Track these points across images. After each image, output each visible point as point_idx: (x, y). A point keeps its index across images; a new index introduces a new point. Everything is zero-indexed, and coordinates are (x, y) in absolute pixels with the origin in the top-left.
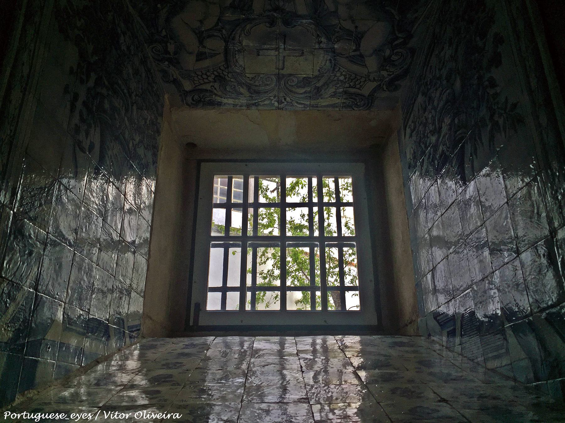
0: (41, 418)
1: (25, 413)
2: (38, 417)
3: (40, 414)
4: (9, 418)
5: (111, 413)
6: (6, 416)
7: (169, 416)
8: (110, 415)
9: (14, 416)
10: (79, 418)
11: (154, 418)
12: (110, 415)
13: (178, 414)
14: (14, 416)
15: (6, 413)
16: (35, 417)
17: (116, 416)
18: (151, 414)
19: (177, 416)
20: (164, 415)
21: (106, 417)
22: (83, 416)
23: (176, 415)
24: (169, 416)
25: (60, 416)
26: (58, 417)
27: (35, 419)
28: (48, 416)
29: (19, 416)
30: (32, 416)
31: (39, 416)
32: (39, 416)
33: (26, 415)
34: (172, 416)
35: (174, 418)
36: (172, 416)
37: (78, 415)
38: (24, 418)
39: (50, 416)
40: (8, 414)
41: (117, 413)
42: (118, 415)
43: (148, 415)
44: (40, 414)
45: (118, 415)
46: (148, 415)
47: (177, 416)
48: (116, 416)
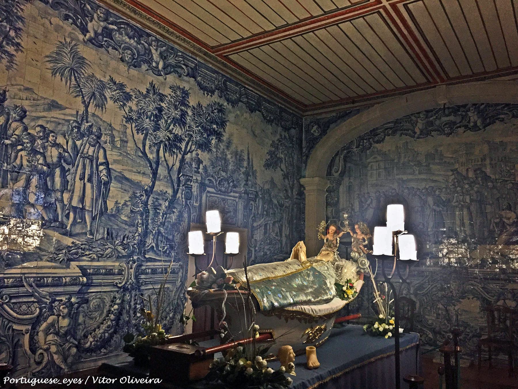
0: (37, 383)
1: (22, 378)
2: (34, 382)
3: (35, 379)
4: (8, 382)
5: (99, 379)
6: (5, 381)
7: (150, 381)
8: (98, 380)
9: (12, 381)
10: (70, 383)
11: (137, 382)
12: (98, 380)
13: (158, 379)
14: (12, 381)
16: (31, 382)
17: (103, 381)
19: (158, 381)
20: (146, 380)
21: (94, 382)
23: (157, 380)
24: (150, 381)
25: (54, 381)
26: (52, 382)
27: (31, 383)
28: (43, 381)
31: (35, 381)
32: (35, 381)
34: (153, 381)
35: (155, 383)
36: (153, 381)
37: (69, 380)
38: (22, 383)
39: (45, 381)
40: (7, 379)
41: (104, 378)
42: (105, 380)
43: (132, 380)
45: (105, 380)
46: (132, 380)
47: (158, 381)
48: (103, 381)
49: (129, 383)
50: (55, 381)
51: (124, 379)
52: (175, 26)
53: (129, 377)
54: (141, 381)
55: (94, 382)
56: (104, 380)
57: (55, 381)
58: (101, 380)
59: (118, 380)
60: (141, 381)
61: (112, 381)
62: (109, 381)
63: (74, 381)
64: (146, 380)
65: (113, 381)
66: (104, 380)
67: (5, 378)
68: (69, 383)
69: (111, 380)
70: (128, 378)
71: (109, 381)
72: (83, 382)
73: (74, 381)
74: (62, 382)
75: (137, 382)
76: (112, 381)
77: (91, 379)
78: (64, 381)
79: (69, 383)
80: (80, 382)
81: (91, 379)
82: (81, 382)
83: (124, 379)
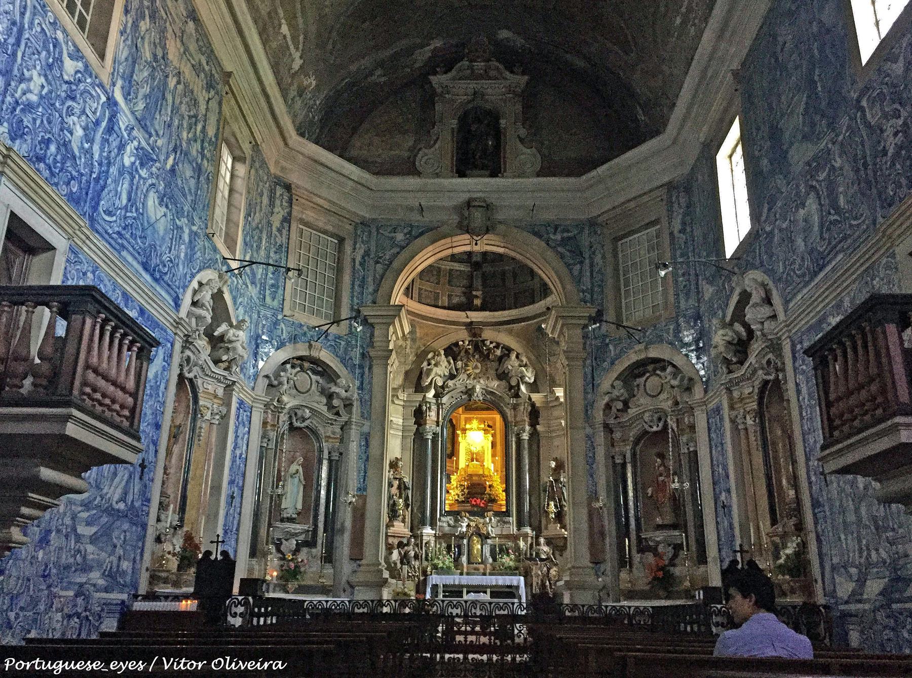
1: (38, 660)
2: (59, 667)
3: (61, 662)
5: (174, 661)
6: (7, 665)
7: (266, 665)
8: (173, 664)
9: (20, 665)
10: (124, 668)
11: (242, 668)
12: (173, 664)
13: (280, 663)
14: (20, 665)
15: (7, 660)
16: (54, 666)
17: (182, 665)
18: (237, 663)
19: (280, 665)
20: (259, 664)
21: (166, 668)
22: (130, 666)
23: (277, 664)
24: (266, 665)
25: (94, 665)
26: (90, 667)
27: (54, 669)
29: (28, 665)
31: (61, 666)
32: (61, 666)
33: (40, 664)
36: (271, 665)
38: (37, 668)
39: (78, 666)
40: (11, 661)
41: (183, 661)
42: (185, 664)
44: (61, 662)
45: (185, 664)
47: (280, 665)
48: (182, 665)
50: (96, 666)
51: (220, 662)
53: (228, 658)
54: (250, 665)
55: (166, 668)
56: (183, 665)
57: (96, 666)
58: (179, 663)
60: (250, 665)
61: (197, 666)
62: (192, 665)
63: (131, 665)
64: (259, 664)
65: (200, 665)
66: (183, 665)
67: (7, 660)
68: (121, 668)
69: (195, 664)
70: (225, 660)
71: (192, 665)
72: (146, 669)
74: (109, 669)
75: (242, 668)
77: (160, 662)
79: (121, 668)
80: (141, 666)
82: (142, 667)
83: (220, 662)
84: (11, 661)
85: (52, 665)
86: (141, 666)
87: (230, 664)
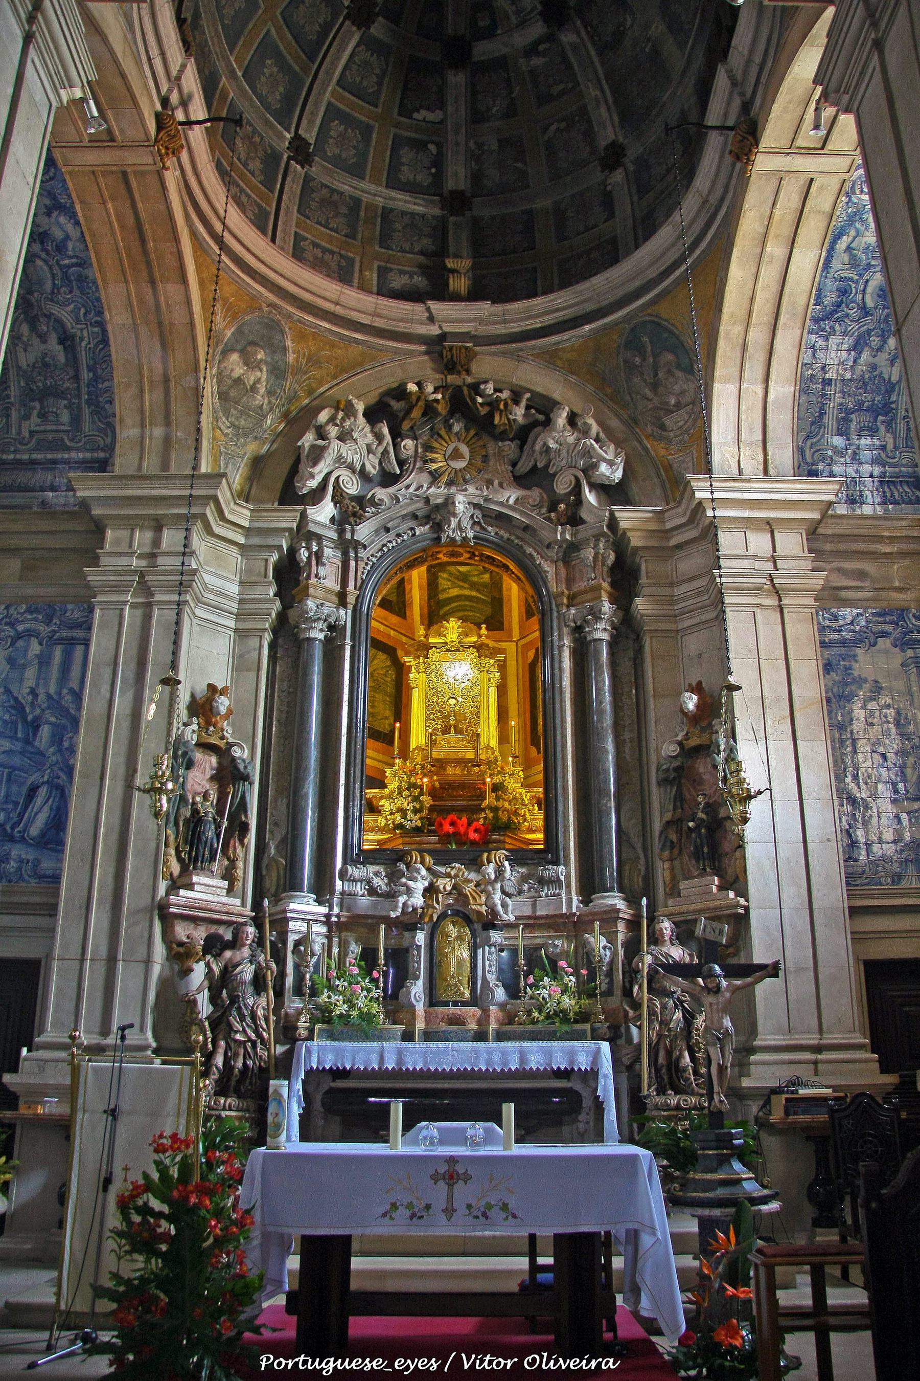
0: (335, 1368)
1: (302, 1358)
2: (329, 1366)
3: (332, 1360)
4: (269, 1367)
6: (264, 1363)
7: (593, 1364)
8: (474, 1362)
9: (279, 1364)
10: (412, 1367)
11: (563, 1367)
12: (474, 1362)
13: (612, 1360)
14: (279, 1364)
15: (264, 1357)
16: (323, 1365)
17: (486, 1363)
18: (556, 1361)
19: (611, 1364)
20: (584, 1362)
21: (466, 1367)
22: (420, 1365)
23: (607, 1362)
24: (593, 1364)
25: (374, 1363)
26: (369, 1366)
27: (323, 1369)
29: (290, 1363)
30: (346, 1363)
31: (331, 1365)
32: (331, 1365)
33: (305, 1362)
34: (600, 1364)
36: (600, 1364)
37: (409, 1361)
39: (353, 1365)
40: (268, 1359)
41: (488, 1358)
42: (490, 1363)
44: (332, 1360)
45: (490, 1363)
47: (611, 1364)
48: (486, 1363)
49: (544, 1367)
51: (534, 1360)
52: (861, 73)
53: (545, 1354)
54: (572, 1364)
55: (466, 1367)
56: (487, 1363)
58: (482, 1362)
59: (521, 1362)
60: (572, 1364)
61: (506, 1364)
62: (498, 1364)
63: (421, 1364)
64: (584, 1362)
65: (509, 1363)
66: (487, 1363)
67: (264, 1357)
68: (408, 1367)
69: (503, 1362)
70: (541, 1357)
71: (498, 1364)
72: (441, 1367)
73: (421, 1364)
74: (393, 1367)
75: (563, 1367)
76: (506, 1364)
77: (458, 1361)
78: (396, 1364)
79: (408, 1367)
80: (434, 1365)
81: (458, 1359)
82: (435, 1366)
83: (534, 1360)
84: (268, 1359)
85: (320, 1364)
86: (434, 1365)
87: (547, 1364)
